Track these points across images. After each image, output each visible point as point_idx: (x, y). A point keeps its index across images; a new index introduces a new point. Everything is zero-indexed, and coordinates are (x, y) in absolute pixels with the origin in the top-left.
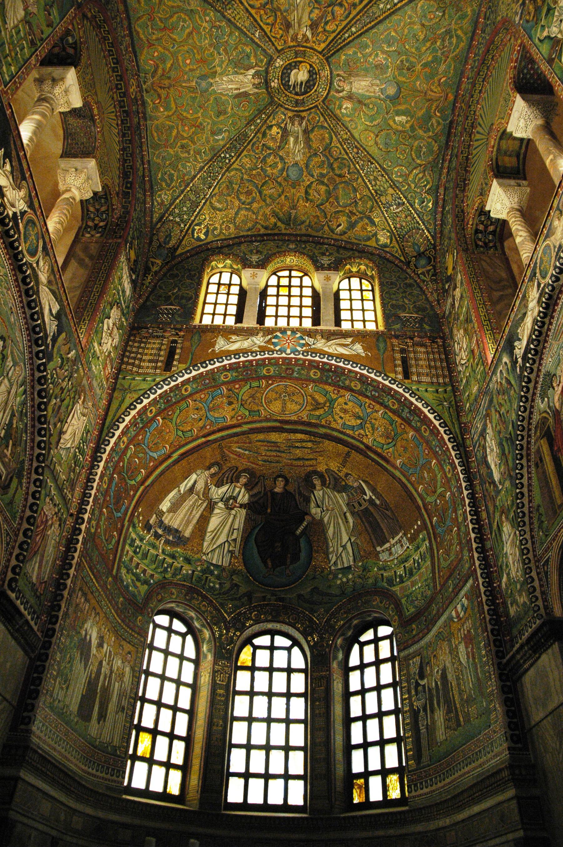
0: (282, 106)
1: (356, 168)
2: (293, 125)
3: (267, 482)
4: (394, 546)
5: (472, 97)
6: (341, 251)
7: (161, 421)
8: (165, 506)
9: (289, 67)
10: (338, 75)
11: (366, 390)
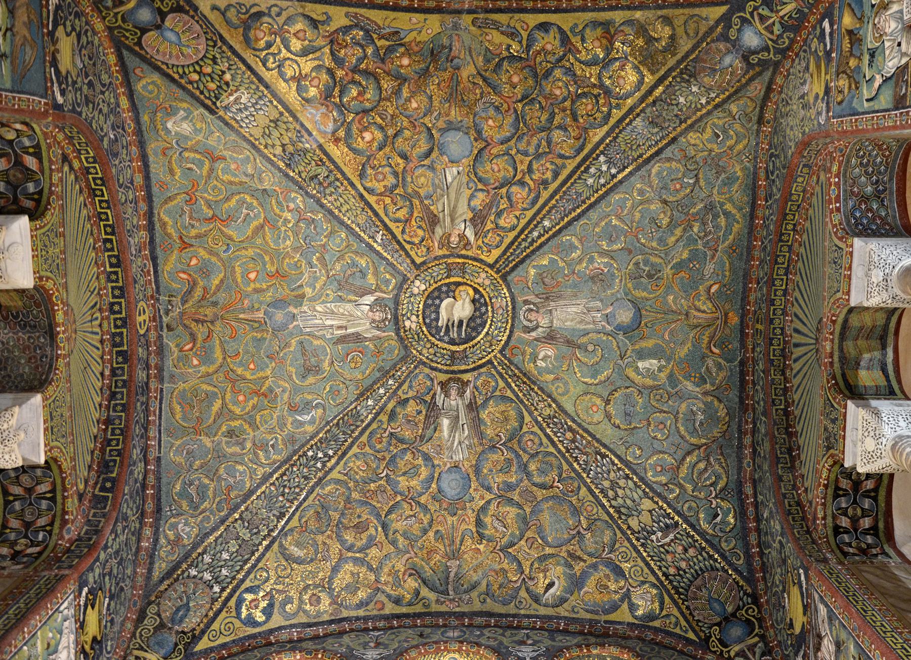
0: (424, 364)
1: (574, 470)
2: (447, 395)
6: (560, 638)
9: (436, 294)
10: (526, 302)
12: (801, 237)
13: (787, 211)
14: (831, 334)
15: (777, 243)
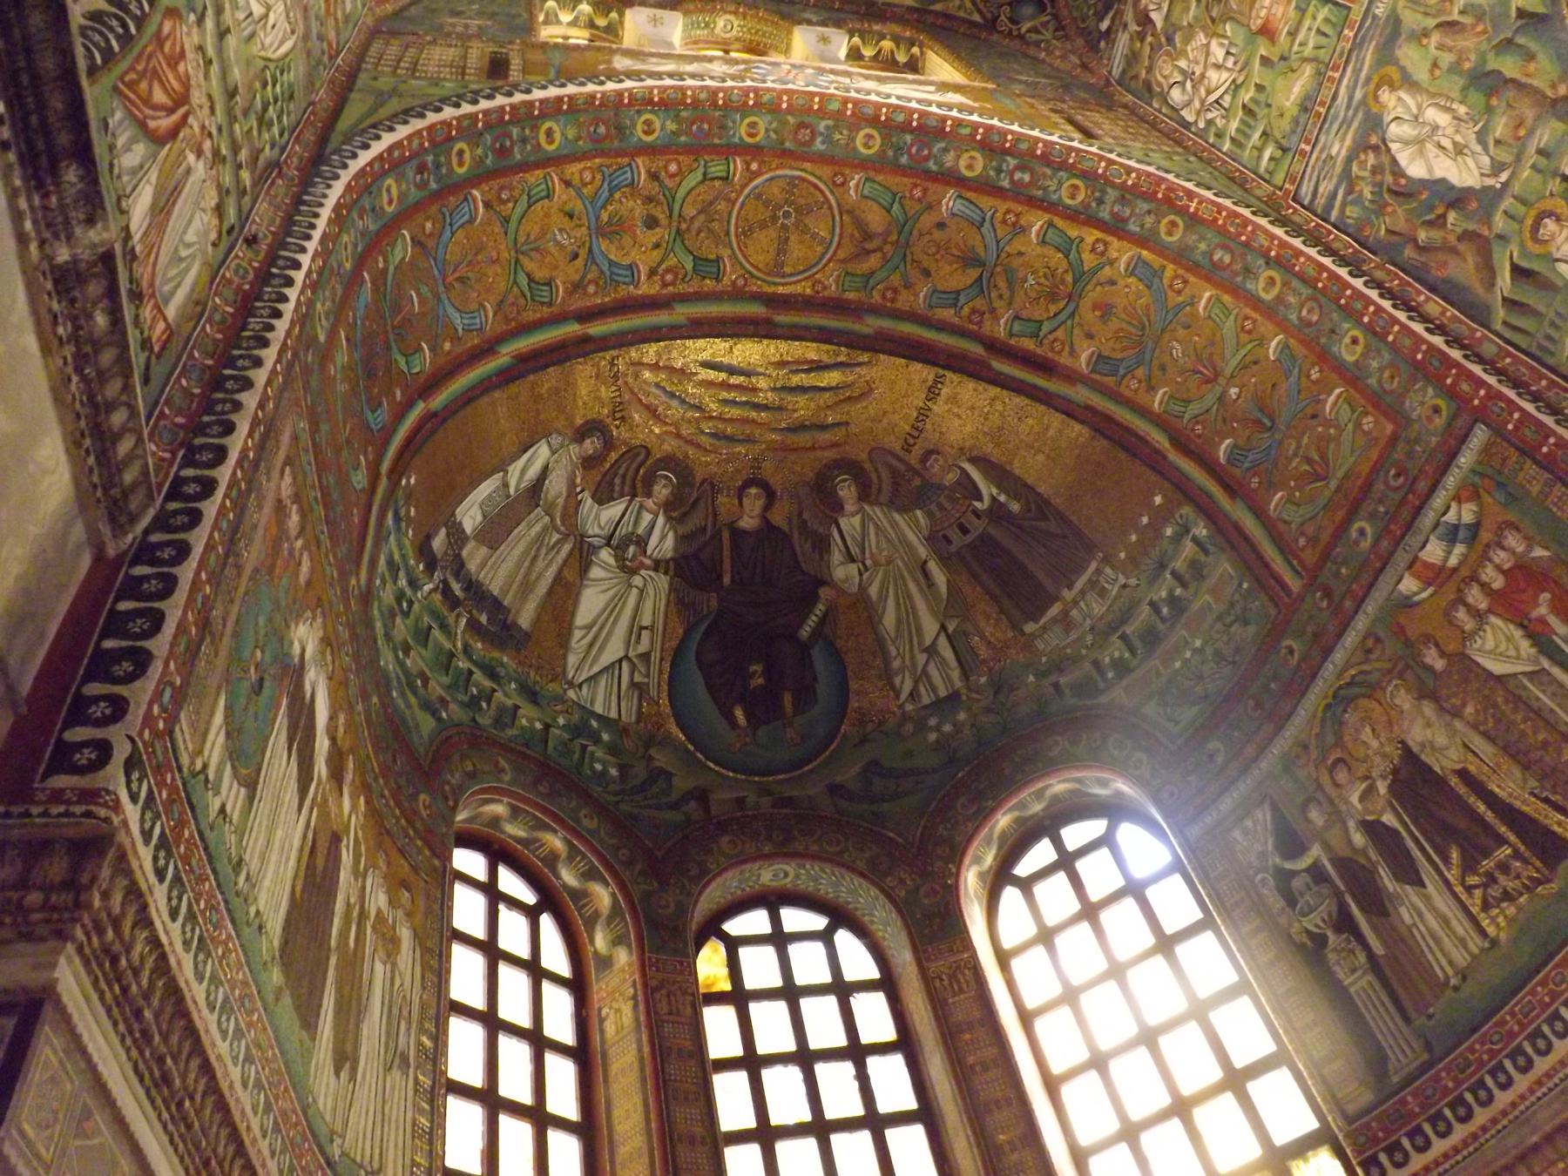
3: (722, 500)
4: (1075, 603)
7: (481, 209)
8: (470, 515)
11: (999, 171)
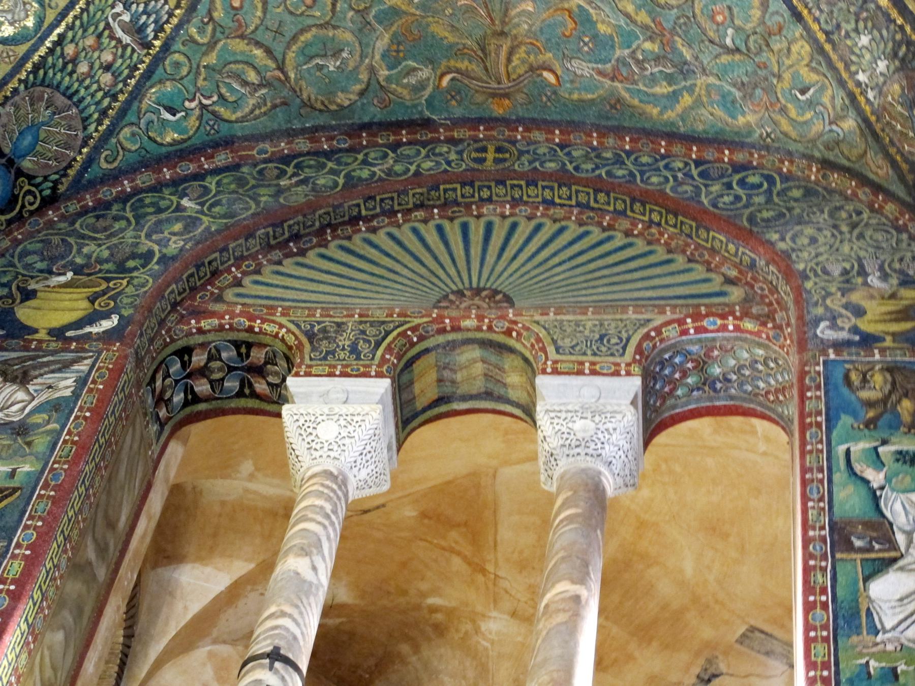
5: (532, 183)
12: (641, 234)
13: (680, 218)
14: (490, 328)
15: (629, 194)
